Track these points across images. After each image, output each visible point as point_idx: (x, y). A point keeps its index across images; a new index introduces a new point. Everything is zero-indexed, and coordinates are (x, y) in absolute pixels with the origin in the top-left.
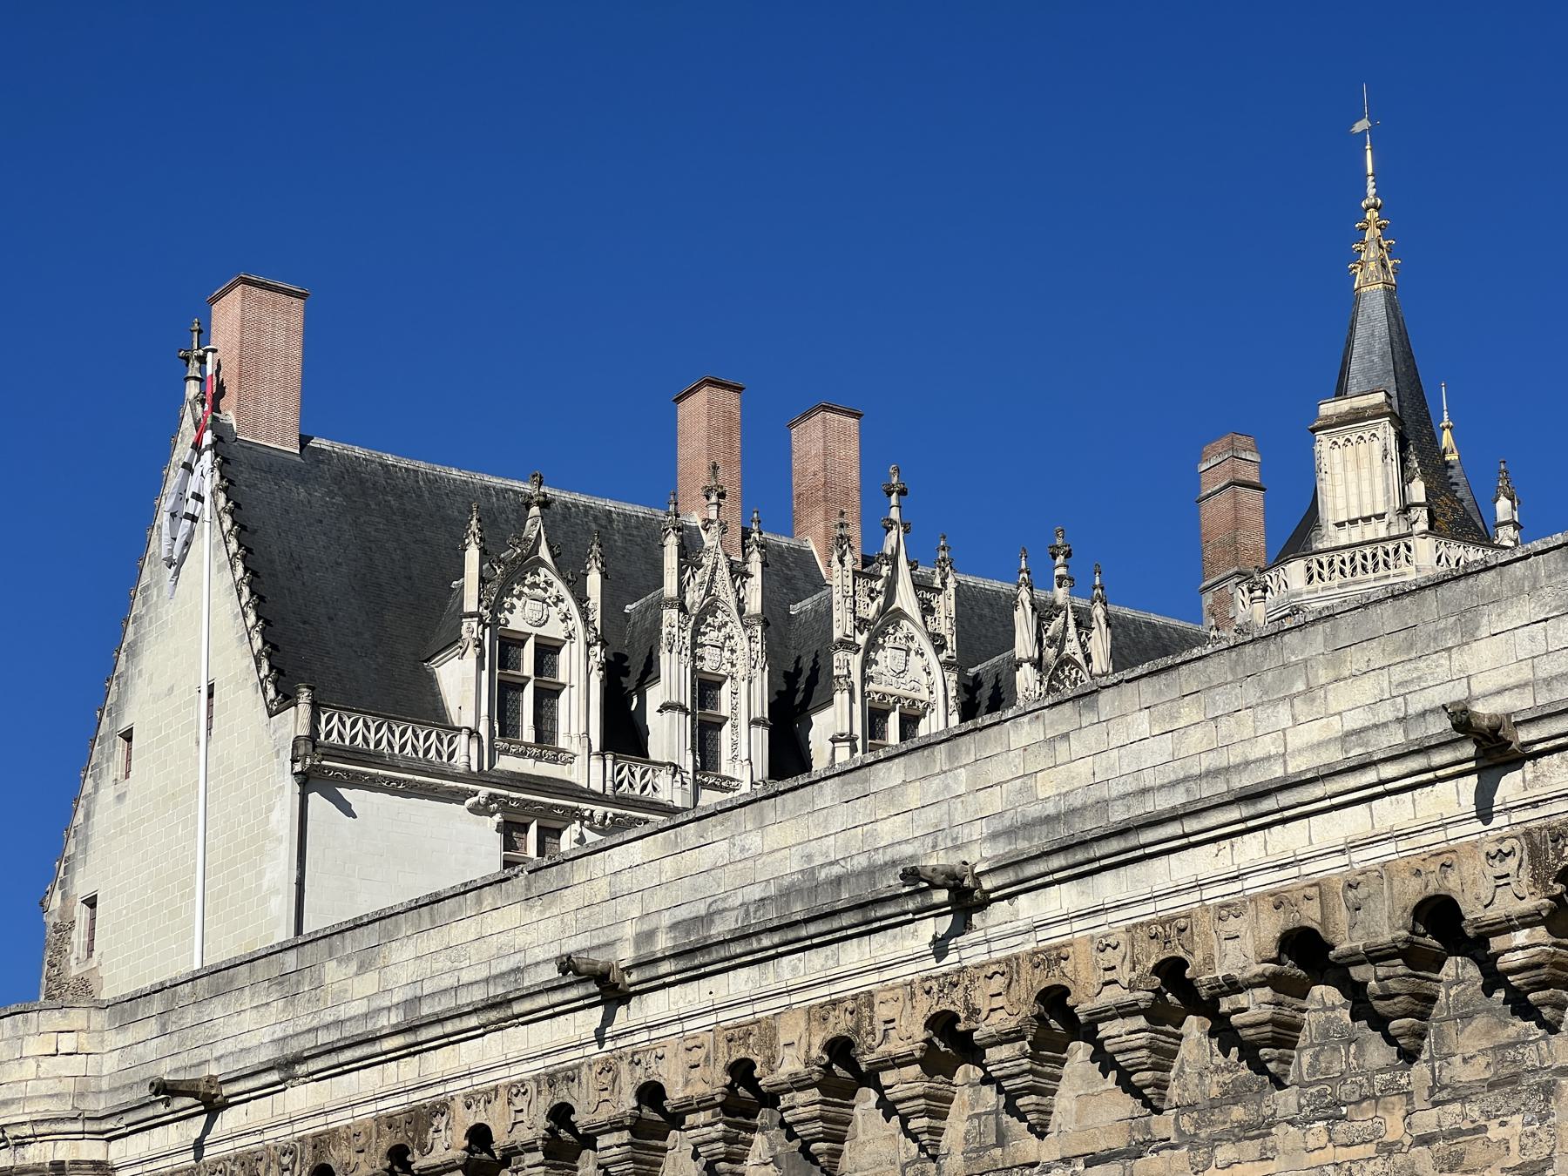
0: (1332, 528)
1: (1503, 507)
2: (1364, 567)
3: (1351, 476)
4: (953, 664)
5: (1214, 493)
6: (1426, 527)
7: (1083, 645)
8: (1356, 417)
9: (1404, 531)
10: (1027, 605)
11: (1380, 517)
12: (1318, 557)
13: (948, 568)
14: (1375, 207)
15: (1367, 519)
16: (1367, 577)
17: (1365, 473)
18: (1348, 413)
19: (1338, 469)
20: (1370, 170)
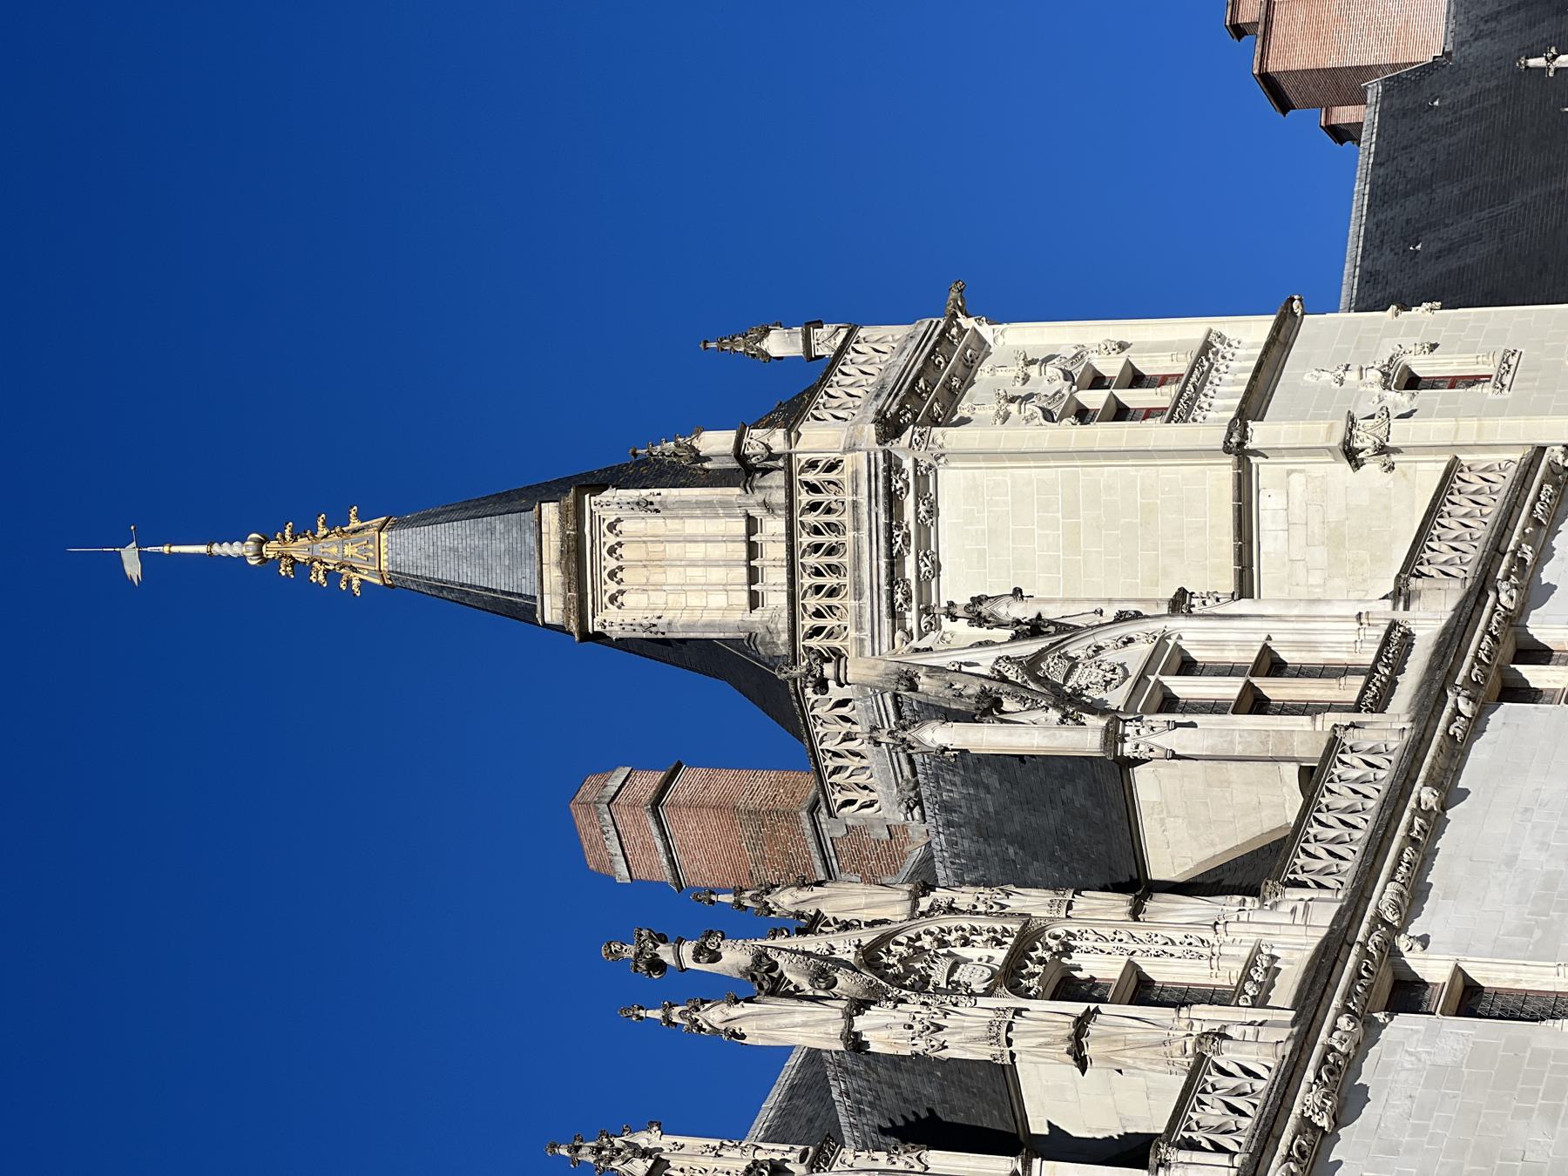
0: (757, 615)
1: (779, 343)
2: (831, 551)
3: (673, 576)
4: (820, 1150)
5: (668, 849)
6: (780, 433)
7: (846, 926)
8: (575, 554)
9: (778, 478)
10: (736, 1011)
11: (752, 524)
12: (800, 635)
13: (618, 1142)
14: (261, 543)
15: (753, 550)
16: (849, 546)
17: (673, 550)
18: (566, 571)
19: (658, 598)
20: (202, 549)
